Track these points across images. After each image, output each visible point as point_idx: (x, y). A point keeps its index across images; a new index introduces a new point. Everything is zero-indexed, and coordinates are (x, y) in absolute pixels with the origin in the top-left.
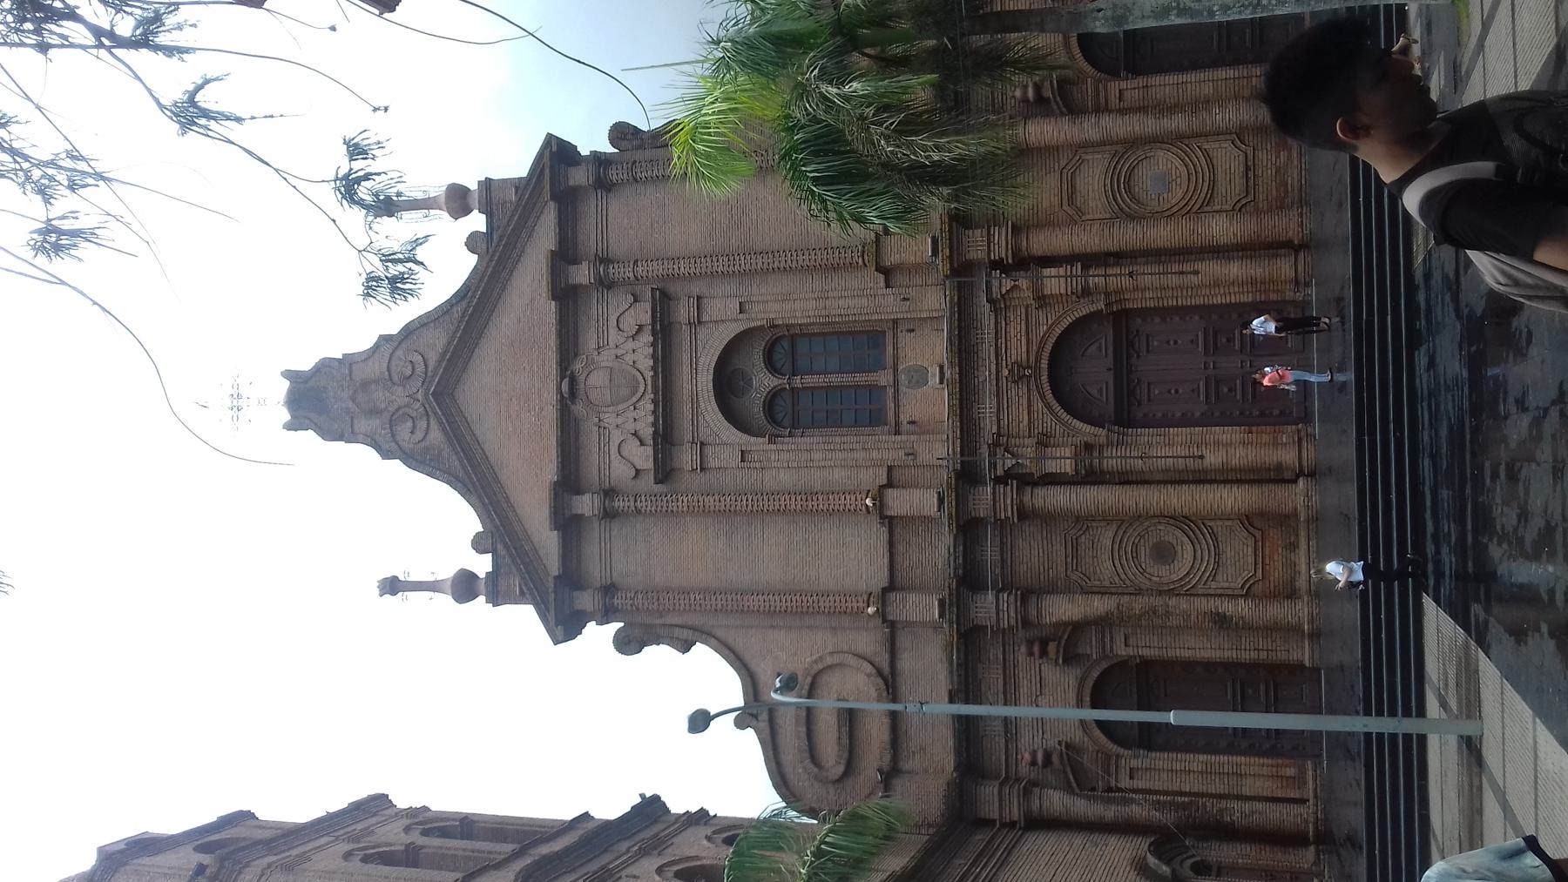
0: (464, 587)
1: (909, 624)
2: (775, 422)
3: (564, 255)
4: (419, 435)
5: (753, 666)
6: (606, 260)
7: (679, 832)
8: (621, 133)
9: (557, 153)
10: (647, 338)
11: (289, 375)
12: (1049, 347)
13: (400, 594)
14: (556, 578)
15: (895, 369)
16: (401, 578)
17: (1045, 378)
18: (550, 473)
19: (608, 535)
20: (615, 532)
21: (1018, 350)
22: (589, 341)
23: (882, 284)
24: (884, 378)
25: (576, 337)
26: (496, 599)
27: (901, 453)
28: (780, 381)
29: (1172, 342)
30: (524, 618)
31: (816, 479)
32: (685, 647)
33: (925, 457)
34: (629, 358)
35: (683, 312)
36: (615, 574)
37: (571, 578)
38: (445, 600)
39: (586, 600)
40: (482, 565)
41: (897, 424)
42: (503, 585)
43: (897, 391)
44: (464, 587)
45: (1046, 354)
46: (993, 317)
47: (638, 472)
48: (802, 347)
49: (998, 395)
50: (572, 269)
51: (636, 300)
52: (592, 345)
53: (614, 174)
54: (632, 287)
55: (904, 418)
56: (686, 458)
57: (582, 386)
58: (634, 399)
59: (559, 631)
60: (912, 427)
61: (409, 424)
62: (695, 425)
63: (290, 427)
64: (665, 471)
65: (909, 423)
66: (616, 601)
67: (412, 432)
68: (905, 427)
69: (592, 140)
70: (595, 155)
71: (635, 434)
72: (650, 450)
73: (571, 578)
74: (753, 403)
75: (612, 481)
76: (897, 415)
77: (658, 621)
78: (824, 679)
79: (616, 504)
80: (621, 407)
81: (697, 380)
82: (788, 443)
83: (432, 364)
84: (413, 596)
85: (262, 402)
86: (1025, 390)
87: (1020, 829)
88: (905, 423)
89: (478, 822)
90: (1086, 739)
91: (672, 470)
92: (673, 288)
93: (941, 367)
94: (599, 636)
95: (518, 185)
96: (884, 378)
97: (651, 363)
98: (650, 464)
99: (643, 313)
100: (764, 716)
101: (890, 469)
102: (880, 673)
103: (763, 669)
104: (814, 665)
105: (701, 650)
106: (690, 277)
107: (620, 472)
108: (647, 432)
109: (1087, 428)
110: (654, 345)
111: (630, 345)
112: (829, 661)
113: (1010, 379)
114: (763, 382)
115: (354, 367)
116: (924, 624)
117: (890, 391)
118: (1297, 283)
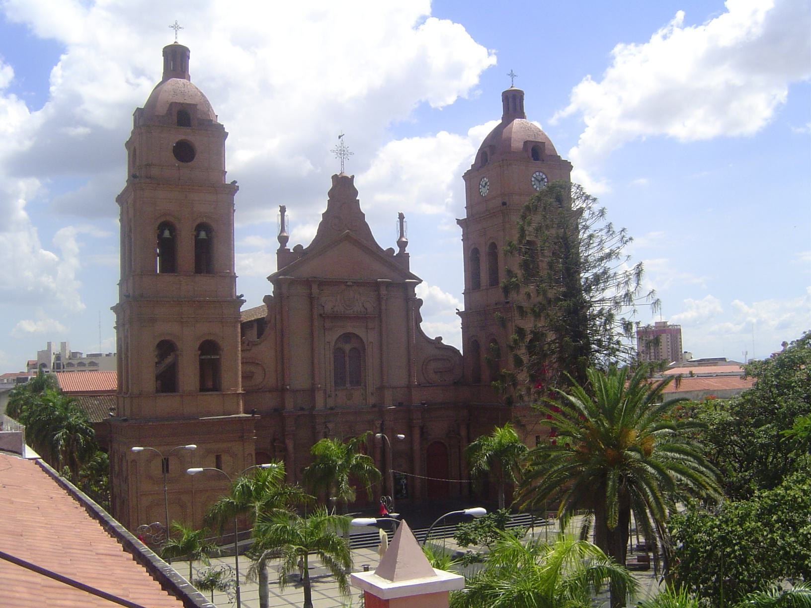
0: (283, 240)
11: (353, 177)
24: (348, 385)
40: (290, 246)
44: (283, 240)
81: (351, 327)
96: (348, 385)
100: (248, 348)
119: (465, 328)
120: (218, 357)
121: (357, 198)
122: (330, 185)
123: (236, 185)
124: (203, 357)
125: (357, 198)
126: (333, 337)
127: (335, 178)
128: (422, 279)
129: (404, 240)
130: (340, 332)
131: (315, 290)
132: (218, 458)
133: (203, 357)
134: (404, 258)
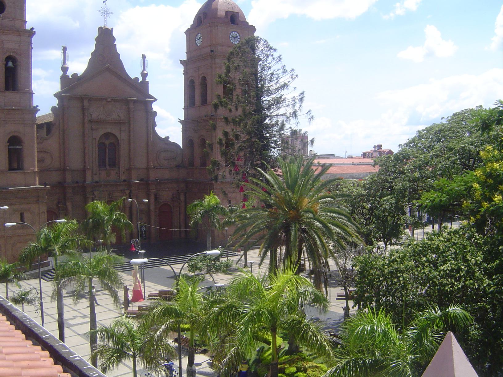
0: (65, 69)
11: (112, 29)
40: (70, 74)
84: (62, 54)
96: (108, 167)
114: (107, 142)
119: (184, 131)
120: (21, 147)
121: (115, 44)
122: (97, 34)
123: (34, 30)
124: (11, 147)
125: (115, 44)
127: (100, 29)
128: (157, 99)
129: (145, 72)
130: (102, 132)
131: (86, 103)
132: (22, 215)
133: (11, 147)
134: (145, 84)
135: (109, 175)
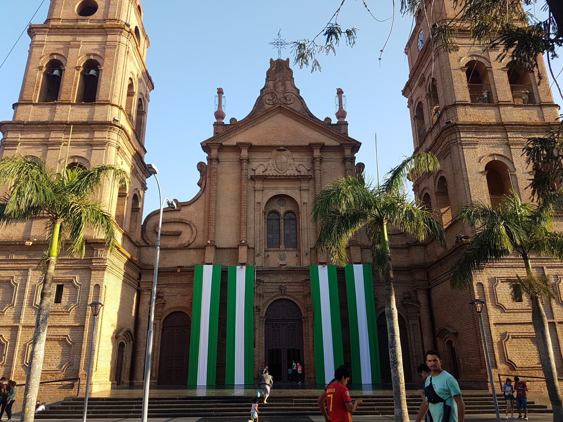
1: (204, 254)
2: (270, 213)
3: (323, 147)
4: (267, 102)
5: (192, 205)
6: (321, 161)
7: (139, 180)
8: (361, 166)
9: (356, 146)
10: (296, 173)
12: (291, 299)
13: (218, 95)
14: (221, 144)
15: (285, 250)
16: (223, 96)
17: (281, 297)
18: (255, 143)
19: (235, 161)
20: (235, 163)
21: (289, 289)
22: (296, 155)
23: (312, 247)
24: (282, 247)
25: (297, 152)
26: (215, 124)
27: (259, 252)
28: (282, 215)
29: (292, 338)
30: (210, 134)
31: (251, 225)
32: (199, 184)
33: (257, 259)
34: (290, 168)
35: (304, 185)
36: (222, 163)
37: (222, 148)
38: (215, 109)
39: (214, 152)
40: (226, 121)
41: (268, 251)
42: (220, 127)
43: (277, 251)
44: (219, 115)
45: (288, 298)
46: (301, 281)
47: (255, 170)
48: (293, 222)
49: (276, 282)
50: (319, 150)
51: (308, 170)
52: (294, 156)
53: (348, 163)
54: (313, 169)
55: (270, 253)
56: (259, 185)
57: (282, 153)
58: (277, 170)
59: (204, 144)
60: (266, 255)
61: (271, 99)
62: (269, 188)
63: (271, 60)
64: (253, 178)
65: (268, 255)
66: (214, 162)
67: (268, 100)
68: (267, 253)
69: (359, 157)
70: (355, 158)
71: (266, 170)
72: (261, 174)
73: (222, 148)
74: (276, 206)
75: (252, 162)
76: (271, 251)
77: (207, 176)
78: (188, 227)
79: (244, 163)
80: (275, 165)
81: (282, 189)
82: (262, 217)
83: (290, 106)
85: (279, 52)
86: (277, 291)
87: (138, 288)
88: (268, 253)
89: (144, 116)
90: (166, 309)
91: (255, 181)
92: (311, 181)
93: (285, 265)
94: (203, 157)
95: (346, 133)
96: (282, 247)
97: (288, 175)
98: (257, 174)
99: (304, 172)
101: (254, 248)
102: (189, 245)
103: (191, 208)
104: (192, 224)
105: (198, 189)
106: (315, 188)
107: (254, 165)
108: (267, 173)
109: (265, 310)
110: (294, 176)
111: (294, 168)
112: (194, 229)
113: (281, 286)
114: (282, 210)
115: (289, 81)
116: (204, 258)
117: (278, 249)
118: (310, 379)
126: (263, 198)
135: (282, 258)
